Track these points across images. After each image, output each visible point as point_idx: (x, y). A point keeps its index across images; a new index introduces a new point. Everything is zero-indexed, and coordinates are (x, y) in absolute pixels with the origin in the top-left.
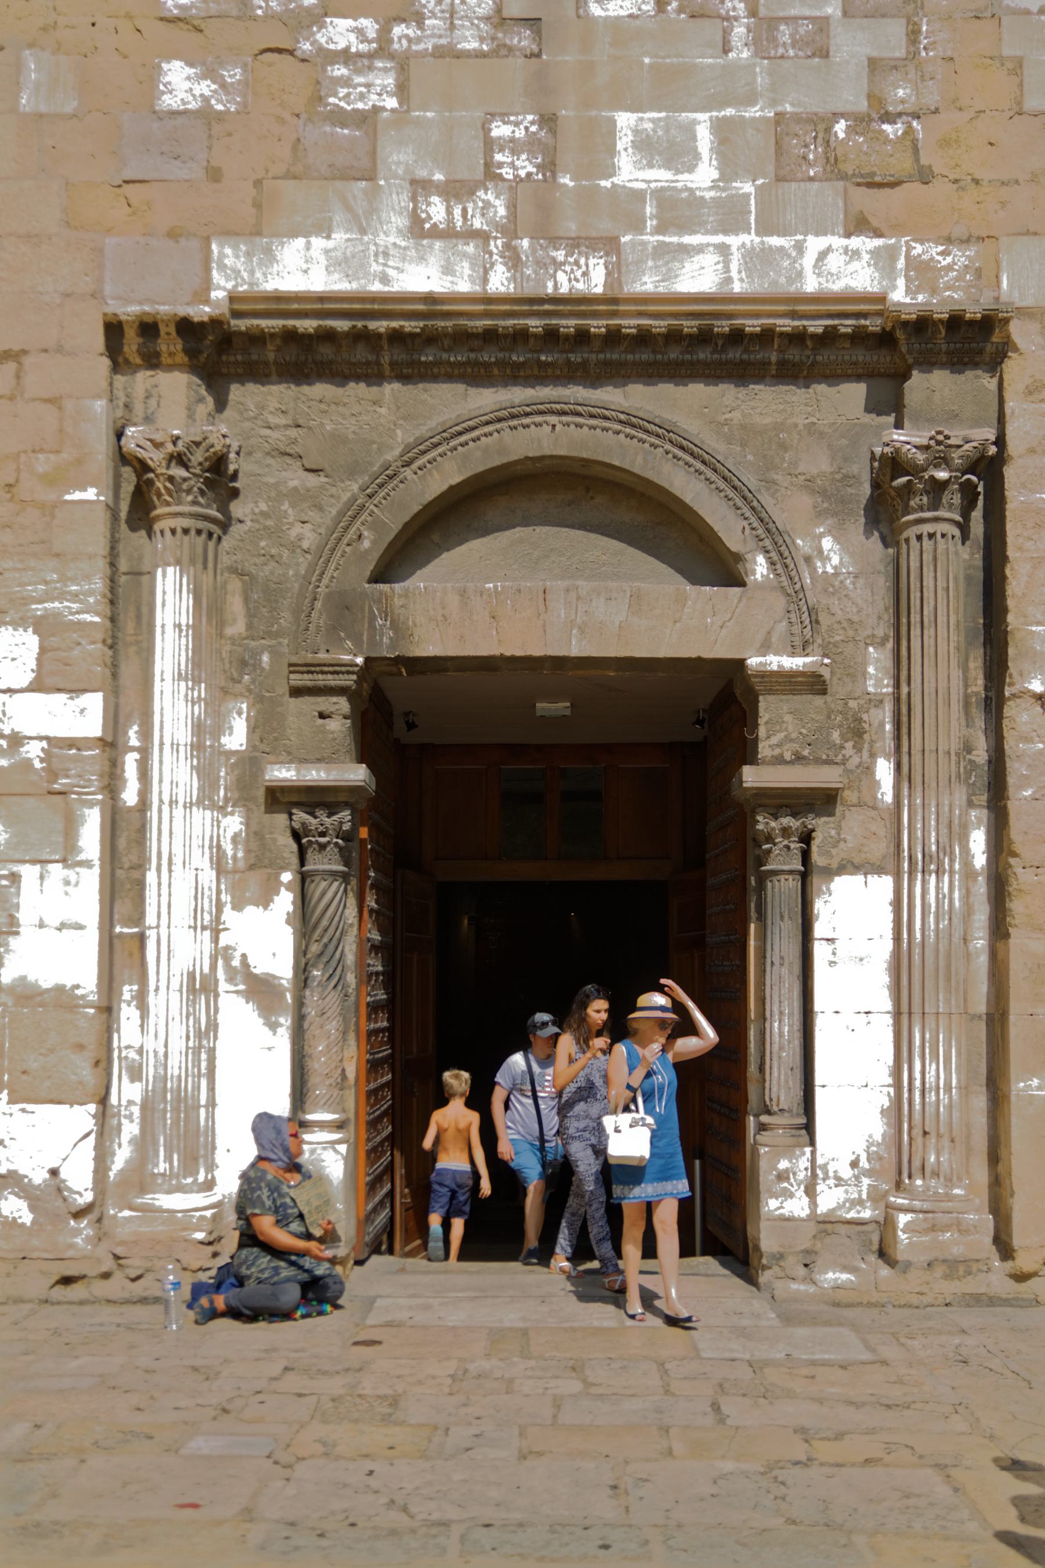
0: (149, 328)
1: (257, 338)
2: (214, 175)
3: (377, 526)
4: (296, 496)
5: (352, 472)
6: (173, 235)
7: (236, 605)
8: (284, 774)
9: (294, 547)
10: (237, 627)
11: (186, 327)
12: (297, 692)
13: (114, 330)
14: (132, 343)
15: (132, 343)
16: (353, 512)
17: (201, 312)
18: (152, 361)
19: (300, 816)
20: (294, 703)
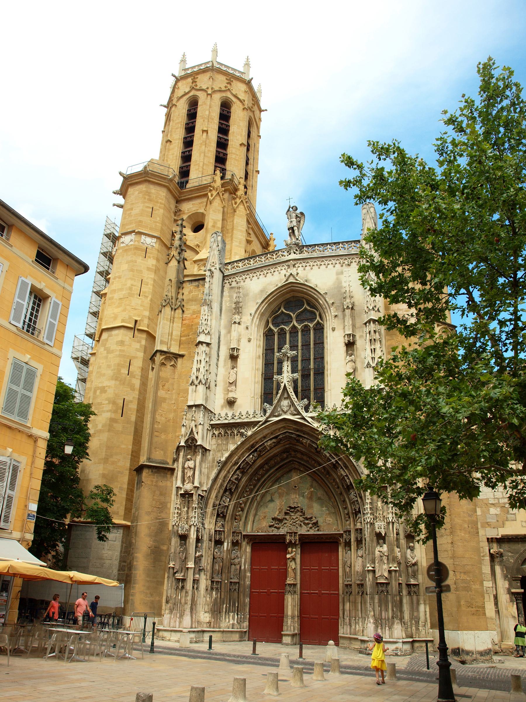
0: (492, 538)
1: (504, 538)
2: (498, 521)
3: (521, 560)
4: (510, 556)
5: (517, 553)
6: (494, 528)
7: (505, 569)
8: (513, 590)
9: (511, 562)
10: (505, 572)
11: (496, 538)
12: (513, 580)
13: (488, 539)
14: (490, 540)
15: (490, 540)
16: (517, 558)
17: (498, 537)
18: (492, 541)
19: (516, 596)
20: (513, 582)
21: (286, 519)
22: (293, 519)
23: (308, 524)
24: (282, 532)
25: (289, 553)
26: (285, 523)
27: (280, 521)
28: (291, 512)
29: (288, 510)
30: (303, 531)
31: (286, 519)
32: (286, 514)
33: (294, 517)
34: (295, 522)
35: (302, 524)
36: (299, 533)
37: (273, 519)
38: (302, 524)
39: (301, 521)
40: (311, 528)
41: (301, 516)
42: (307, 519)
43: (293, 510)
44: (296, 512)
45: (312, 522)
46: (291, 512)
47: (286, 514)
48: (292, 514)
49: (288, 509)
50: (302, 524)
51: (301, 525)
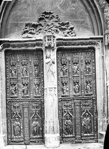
21: (41, 25)
22: (48, 25)
23: (65, 29)
24: (39, 36)
25: (47, 57)
26: (40, 29)
27: (35, 26)
28: (47, 18)
29: (42, 16)
30: (60, 35)
31: (41, 25)
32: (41, 19)
33: (49, 24)
34: (50, 29)
35: (59, 30)
36: (57, 38)
37: (27, 25)
38: (59, 30)
39: (57, 27)
40: (68, 33)
41: (56, 22)
42: (63, 24)
43: (48, 16)
44: (51, 18)
45: (69, 27)
46: (47, 18)
47: (41, 19)
48: (47, 20)
49: (44, 14)
50: (58, 29)
51: (57, 30)
